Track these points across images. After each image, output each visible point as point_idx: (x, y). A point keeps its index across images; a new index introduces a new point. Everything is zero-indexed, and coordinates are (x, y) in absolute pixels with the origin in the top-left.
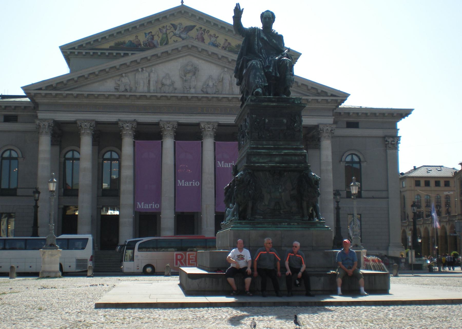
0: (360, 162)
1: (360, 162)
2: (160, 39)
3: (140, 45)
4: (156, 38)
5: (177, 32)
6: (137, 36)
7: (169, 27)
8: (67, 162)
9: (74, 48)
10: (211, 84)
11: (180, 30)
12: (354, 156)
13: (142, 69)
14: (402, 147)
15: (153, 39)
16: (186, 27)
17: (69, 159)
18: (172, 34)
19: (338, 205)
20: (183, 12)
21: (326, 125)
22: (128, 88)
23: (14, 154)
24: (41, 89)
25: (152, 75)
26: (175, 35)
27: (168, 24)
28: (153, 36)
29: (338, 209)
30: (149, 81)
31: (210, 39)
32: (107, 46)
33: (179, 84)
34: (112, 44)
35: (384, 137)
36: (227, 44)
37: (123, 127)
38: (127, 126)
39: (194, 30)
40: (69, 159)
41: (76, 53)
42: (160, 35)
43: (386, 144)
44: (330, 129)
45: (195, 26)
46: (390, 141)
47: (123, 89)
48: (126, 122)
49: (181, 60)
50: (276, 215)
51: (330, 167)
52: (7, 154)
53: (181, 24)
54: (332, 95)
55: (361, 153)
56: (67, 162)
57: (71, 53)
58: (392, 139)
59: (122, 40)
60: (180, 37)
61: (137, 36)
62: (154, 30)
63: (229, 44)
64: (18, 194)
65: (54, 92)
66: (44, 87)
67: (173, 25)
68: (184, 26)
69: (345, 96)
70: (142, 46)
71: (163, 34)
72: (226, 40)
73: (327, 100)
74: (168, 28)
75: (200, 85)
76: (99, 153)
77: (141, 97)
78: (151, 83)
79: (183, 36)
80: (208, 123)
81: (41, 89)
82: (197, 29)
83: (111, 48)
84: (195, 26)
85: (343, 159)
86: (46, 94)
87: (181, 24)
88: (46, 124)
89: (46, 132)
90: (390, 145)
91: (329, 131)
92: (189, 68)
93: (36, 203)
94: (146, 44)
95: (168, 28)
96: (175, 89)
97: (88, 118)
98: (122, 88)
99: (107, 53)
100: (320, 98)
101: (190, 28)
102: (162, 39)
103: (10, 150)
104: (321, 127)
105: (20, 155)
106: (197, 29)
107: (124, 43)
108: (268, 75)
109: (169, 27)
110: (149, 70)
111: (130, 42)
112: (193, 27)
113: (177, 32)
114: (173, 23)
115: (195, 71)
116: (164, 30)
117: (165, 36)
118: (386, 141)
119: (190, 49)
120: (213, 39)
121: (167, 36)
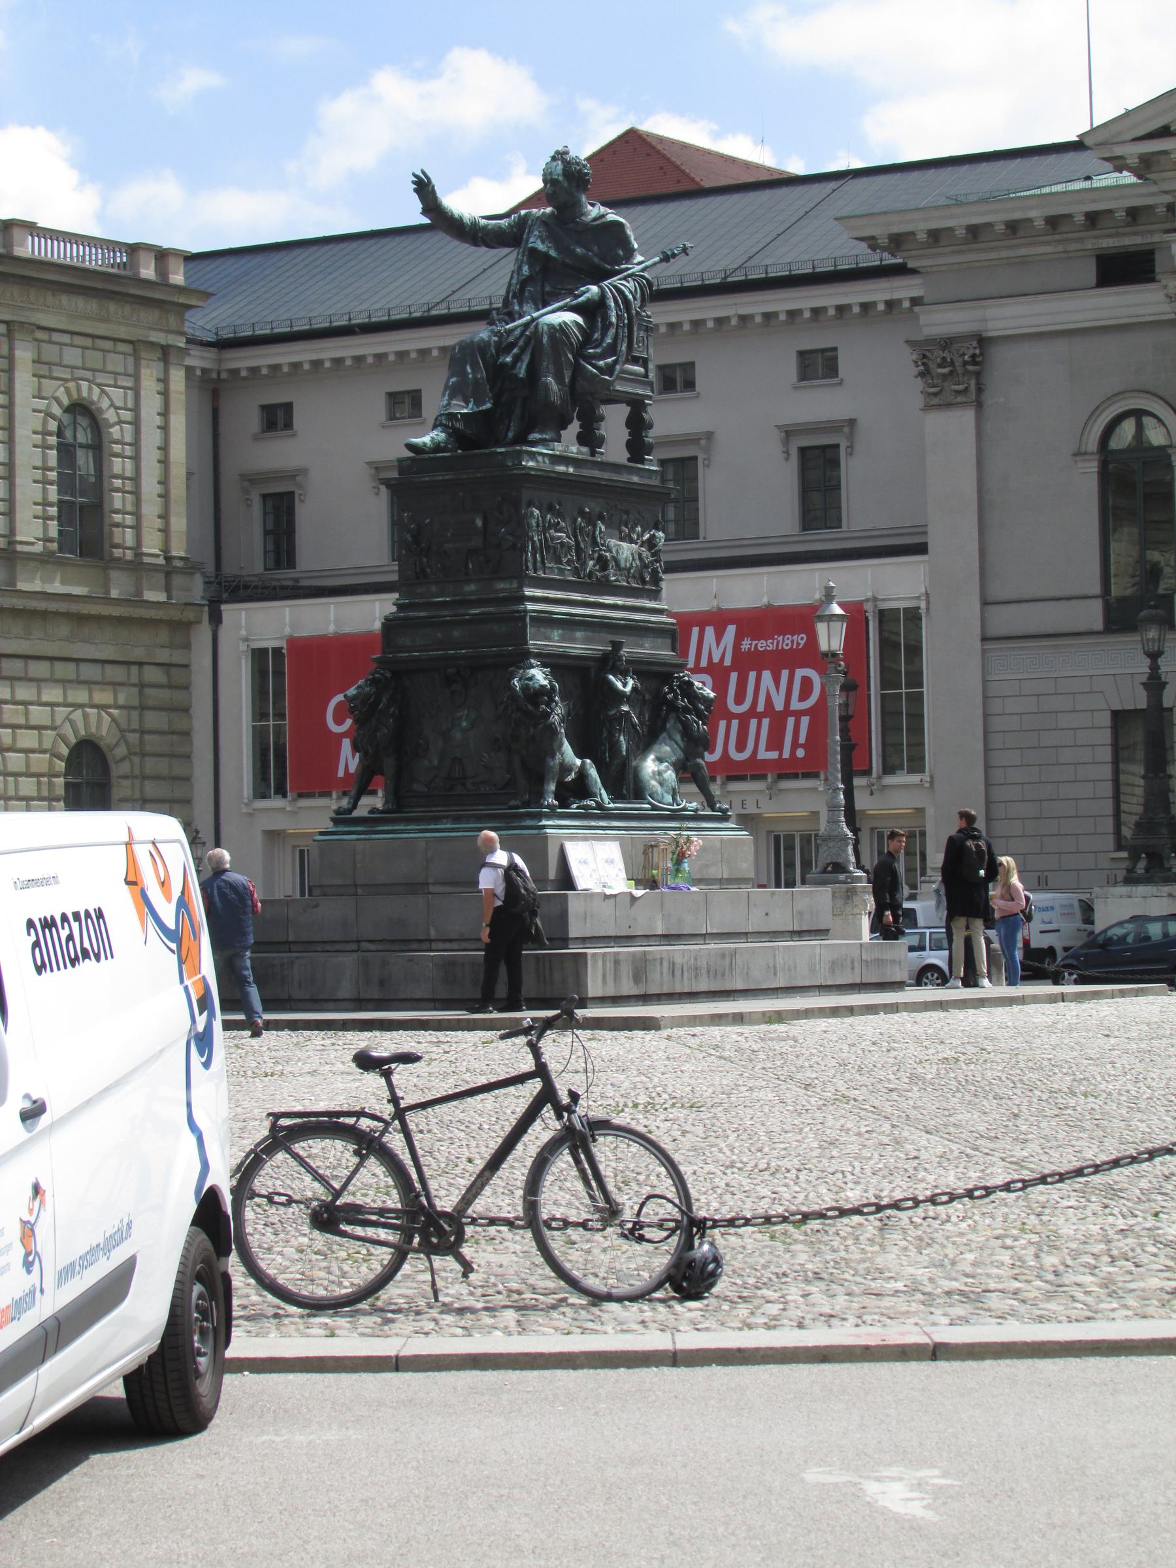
93: (1155, 668)
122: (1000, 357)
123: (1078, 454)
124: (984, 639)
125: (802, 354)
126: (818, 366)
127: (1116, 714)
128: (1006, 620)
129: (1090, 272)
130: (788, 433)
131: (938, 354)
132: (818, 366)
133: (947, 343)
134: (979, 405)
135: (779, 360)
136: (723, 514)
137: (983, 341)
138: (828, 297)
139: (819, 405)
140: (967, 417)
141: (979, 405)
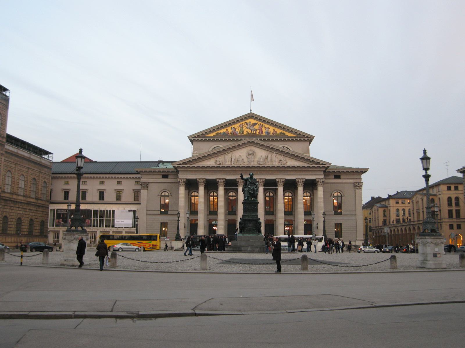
0: (341, 196)
1: (341, 196)
2: (239, 130)
3: (229, 134)
4: (237, 130)
5: (248, 126)
6: (227, 130)
7: (244, 124)
8: (192, 197)
9: (195, 137)
10: (261, 160)
11: (249, 125)
12: (338, 193)
13: (228, 153)
14: (363, 188)
15: (235, 130)
16: (253, 124)
17: (193, 196)
18: (245, 127)
19: (324, 219)
20: (251, 116)
21: (320, 179)
22: (221, 162)
23: (167, 194)
24: (180, 164)
25: (233, 156)
26: (247, 128)
27: (243, 122)
28: (235, 129)
29: (324, 221)
30: (231, 159)
31: (266, 129)
32: (211, 135)
33: (246, 160)
34: (214, 134)
35: (354, 183)
36: (274, 132)
37: (219, 181)
38: (221, 181)
39: (257, 125)
40: (193, 196)
41: (196, 139)
42: (239, 128)
43: (355, 187)
44: (322, 181)
45: (257, 123)
46: (357, 185)
47: (219, 163)
48: (220, 179)
49: (247, 148)
50: (250, 231)
51: (322, 200)
52: (163, 194)
53: (250, 122)
54: (322, 164)
55: (341, 191)
56: (192, 197)
57: (193, 139)
58: (358, 184)
59: (219, 132)
60: (250, 129)
61: (227, 130)
62: (236, 126)
63: (276, 132)
64: (169, 213)
65: (186, 166)
66: (181, 163)
67: (246, 123)
68: (252, 123)
69: (331, 164)
70: (230, 134)
71: (241, 128)
72: (274, 130)
73: (320, 167)
74: (243, 124)
75: (256, 159)
76: (208, 193)
77: (228, 167)
78: (232, 159)
79: (251, 128)
80: (260, 179)
81: (180, 164)
82: (259, 125)
83: (214, 136)
84: (257, 123)
85: (332, 195)
86: (183, 167)
87: (250, 122)
88: (183, 180)
89: (183, 185)
90: (357, 187)
91: (322, 182)
92: (251, 152)
93: (179, 219)
94: (232, 133)
95: (243, 124)
96: (244, 162)
97: (202, 177)
98: (218, 163)
99: (212, 139)
100: (316, 166)
101: (255, 124)
102: (240, 130)
103: (165, 192)
104: (317, 180)
105: (170, 195)
106: (259, 125)
107: (220, 133)
108: (250, 193)
109: (244, 124)
110: (231, 153)
111: (224, 132)
112: (256, 124)
113: (248, 126)
114: (246, 121)
115: (253, 154)
116: (241, 126)
117: (242, 129)
118: (355, 185)
119: (251, 143)
120: (267, 130)
121: (243, 129)
122: (150, 185)
123: (158, 196)
124: (147, 214)
125: (117, 181)
126: (119, 183)
127: (161, 223)
128: (149, 212)
129: (161, 176)
130: (99, 190)
131: (143, 184)
132: (119, 183)
133: (144, 183)
134: (147, 190)
135: (115, 181)
136: (89, 198)
137: (148, 183)
138: (104, 176)
139: (119, 187)
140: (146, 190)
141: (147, 190)
